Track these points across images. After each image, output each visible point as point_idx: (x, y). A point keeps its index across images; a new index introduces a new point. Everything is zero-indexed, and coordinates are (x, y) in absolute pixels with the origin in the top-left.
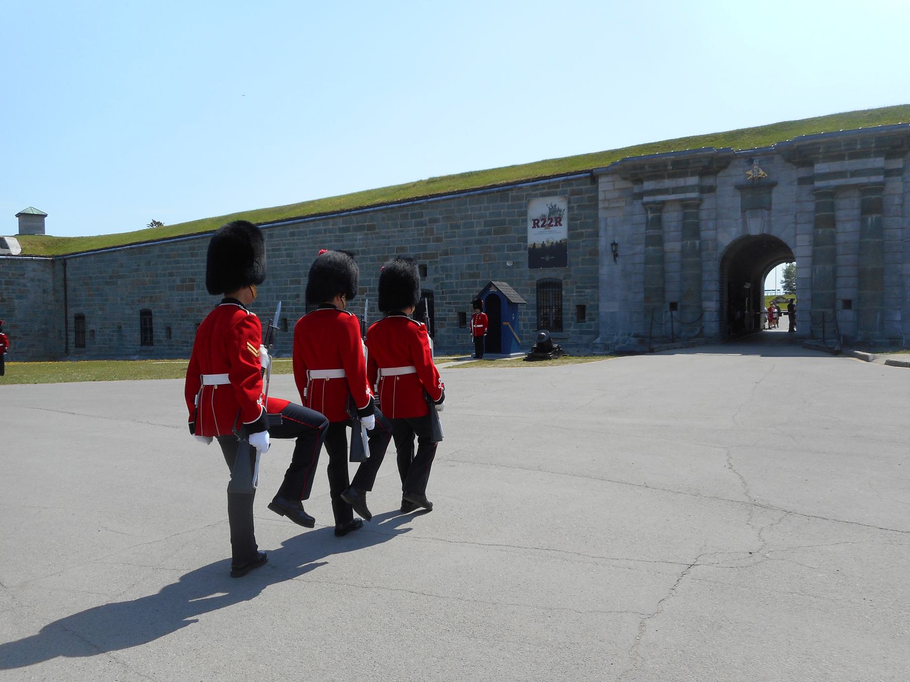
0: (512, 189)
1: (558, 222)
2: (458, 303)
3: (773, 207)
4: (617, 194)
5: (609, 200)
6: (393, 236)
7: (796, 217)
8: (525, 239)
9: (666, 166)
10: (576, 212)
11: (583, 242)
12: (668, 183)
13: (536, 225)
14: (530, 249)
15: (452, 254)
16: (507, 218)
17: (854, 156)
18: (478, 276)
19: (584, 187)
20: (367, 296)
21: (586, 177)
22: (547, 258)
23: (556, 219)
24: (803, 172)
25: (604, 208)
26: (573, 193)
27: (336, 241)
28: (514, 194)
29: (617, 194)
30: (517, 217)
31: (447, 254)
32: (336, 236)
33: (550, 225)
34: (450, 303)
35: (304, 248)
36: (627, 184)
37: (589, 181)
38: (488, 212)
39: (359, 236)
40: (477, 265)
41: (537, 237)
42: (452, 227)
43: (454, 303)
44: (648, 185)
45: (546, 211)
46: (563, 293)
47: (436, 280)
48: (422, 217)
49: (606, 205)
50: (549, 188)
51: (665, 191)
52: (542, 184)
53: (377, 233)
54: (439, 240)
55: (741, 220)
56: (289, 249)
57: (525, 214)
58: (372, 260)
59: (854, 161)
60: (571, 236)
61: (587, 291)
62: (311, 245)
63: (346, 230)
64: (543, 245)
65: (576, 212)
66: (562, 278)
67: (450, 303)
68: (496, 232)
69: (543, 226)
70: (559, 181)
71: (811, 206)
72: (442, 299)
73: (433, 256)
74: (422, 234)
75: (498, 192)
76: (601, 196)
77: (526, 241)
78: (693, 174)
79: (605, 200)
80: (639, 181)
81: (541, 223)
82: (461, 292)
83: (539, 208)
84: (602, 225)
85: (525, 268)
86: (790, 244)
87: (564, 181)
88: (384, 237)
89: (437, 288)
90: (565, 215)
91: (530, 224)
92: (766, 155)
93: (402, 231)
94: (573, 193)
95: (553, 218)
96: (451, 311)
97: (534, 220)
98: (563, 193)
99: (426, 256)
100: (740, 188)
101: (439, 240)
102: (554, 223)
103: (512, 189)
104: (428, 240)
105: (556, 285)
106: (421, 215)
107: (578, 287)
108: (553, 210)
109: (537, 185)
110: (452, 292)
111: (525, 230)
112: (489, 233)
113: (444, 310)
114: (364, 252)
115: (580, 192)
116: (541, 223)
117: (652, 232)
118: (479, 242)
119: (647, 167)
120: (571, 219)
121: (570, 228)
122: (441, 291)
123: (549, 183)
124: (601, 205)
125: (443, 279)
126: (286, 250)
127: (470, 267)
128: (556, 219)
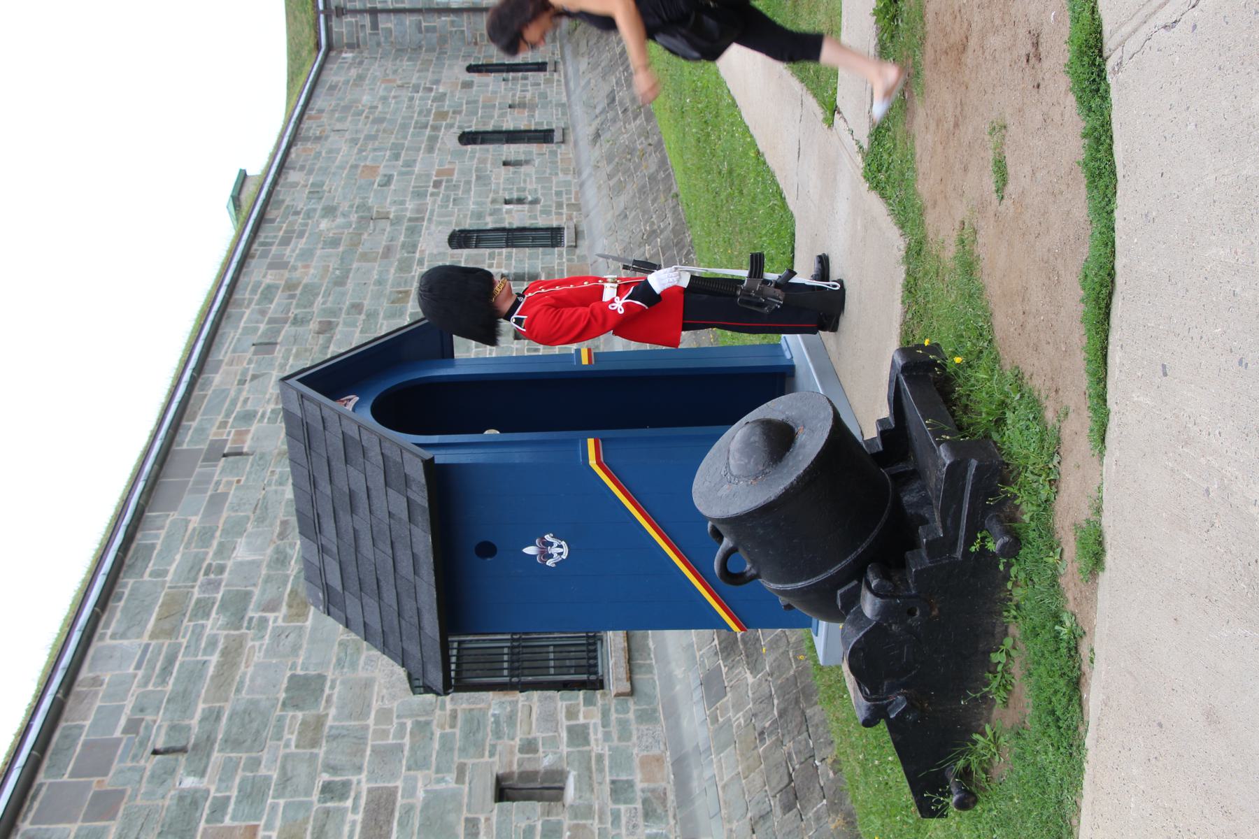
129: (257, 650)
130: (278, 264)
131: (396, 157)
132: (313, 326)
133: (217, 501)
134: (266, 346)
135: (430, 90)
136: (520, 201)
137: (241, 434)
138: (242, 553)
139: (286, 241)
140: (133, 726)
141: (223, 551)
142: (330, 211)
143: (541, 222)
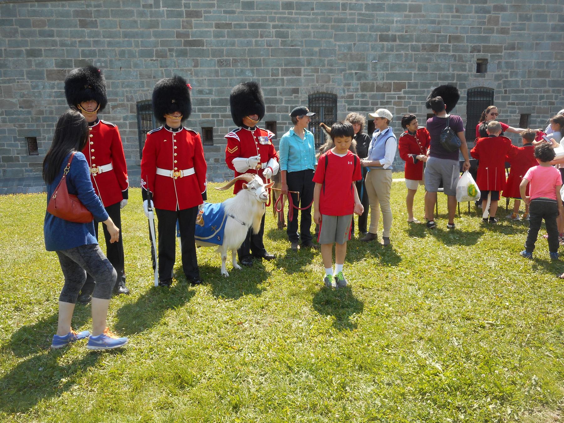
2: (523, 104)
6: (447, 22)
15: (519, 49)
20: (405, 93)
27: (360, 21)
31: (513, 48)
32: (360, 14)
34: (513, 104)
35: (308, 27)
39: (397, 17)
40: (548, 63)
42: (522, 18)
43: (518, 104)
47: (498, 78)
53: (423, 16)
54: (503, 31)
56: (282, 26)
58: (414, 49)
62: (320, 24)
63: (379, 7)
67: (513, 104)
72: (504, 98)
73: (496, 49)
74: (484, 23)
82: (527, 91)
88: (433, 22)
89: (499, 86)
93: (459, 17)
96: (515, 112)
99: (487, 49)
104: (491, 31)
110: (516, 92)
113: (506, 112)
114: (402, 38)
118: (551, 37)
122: (503, 90)
125: (506, 76)
126: (274, 27)
127: (539, 65)
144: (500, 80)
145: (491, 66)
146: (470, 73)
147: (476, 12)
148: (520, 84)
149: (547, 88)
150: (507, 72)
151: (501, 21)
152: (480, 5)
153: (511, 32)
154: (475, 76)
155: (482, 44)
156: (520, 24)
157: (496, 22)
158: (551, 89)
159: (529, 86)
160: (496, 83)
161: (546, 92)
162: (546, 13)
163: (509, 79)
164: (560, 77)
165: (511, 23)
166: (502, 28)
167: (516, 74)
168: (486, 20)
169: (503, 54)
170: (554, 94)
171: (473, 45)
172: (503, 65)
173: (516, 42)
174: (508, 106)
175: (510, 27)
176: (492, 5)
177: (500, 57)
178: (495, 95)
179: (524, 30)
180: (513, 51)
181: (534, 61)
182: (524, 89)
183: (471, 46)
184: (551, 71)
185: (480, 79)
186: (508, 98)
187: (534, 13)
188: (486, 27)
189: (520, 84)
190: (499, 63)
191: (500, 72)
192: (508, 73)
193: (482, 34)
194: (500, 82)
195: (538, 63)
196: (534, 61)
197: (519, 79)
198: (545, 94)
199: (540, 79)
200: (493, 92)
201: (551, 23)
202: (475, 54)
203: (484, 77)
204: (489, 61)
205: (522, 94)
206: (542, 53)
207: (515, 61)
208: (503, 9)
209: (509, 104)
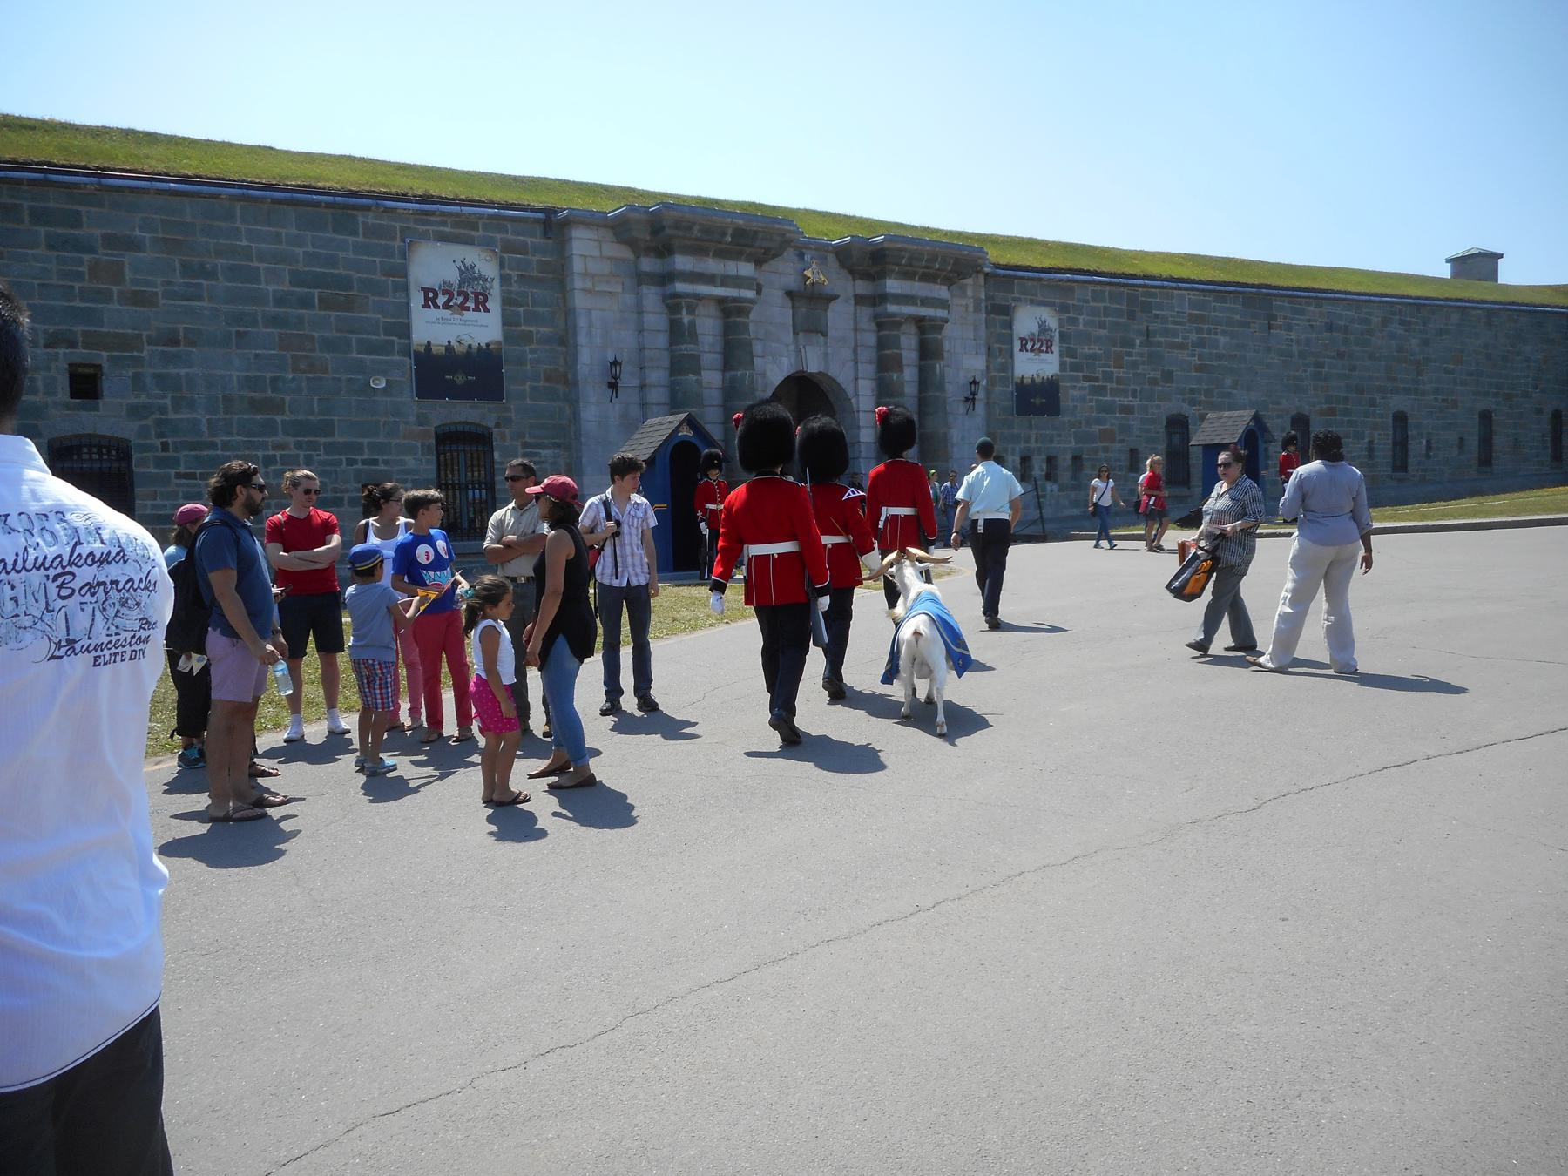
0: (367, 208)
1: (481, 303)
3: (831, 333)
4: (605, 268)
5: (593, 276)
7: (855, 351)
8: (406, 330)
9: (724, 234)
10: (515, 288)
11: (533, 351)
12: (712, 265)
13: (430, 300)
14: (416, 353)
15: (193, 344)
16: (356, 276)
17: (928, 277)
18: (278, 408)
19: (529, 240)
21: (536, 221)
22: (460, 379)
23: (476, 295)
24: (862, 287)
25: (584, 290)
26: (508, 248)
28: (371, 219)
29: (605, 268)
30: (378, 277)
31: (174, 342)
33: (463, 307)
36: (625, 253)
37: (539, 229)
38: (300, 251)
40: (274, 380)
41: (434, 329)
42: (187, 269)
44: (682, 262)
45: (453, 276)
46: (496, 455)
47: (136, 412)
48: (77, 223)
49: (589, 285)
50: (456, 225)
51: (710, 279)
52: (443, 214)
54: (140, 299)
55: (792, 347)
57: (404, 273)
59: (922, 284)
60: (508, 337)
61: (543, 452)
64: (449, 348)
65: (515, 288)
66: (491, 424)
68: (326, 304)
69: (446, 306)
70: (481, 216)
71: (871, 339)
75: (329, 205)
76: (578, 266)
77: (409, 337)
78: (748, 260)
79: (585, 275)
80: (664, 250)
81: (441, 300)
83: (435, 264)
84: (582, 322)
85: (407, 397)
86: (850, 391)
87: (491, 217)
90: (496, 291)
91: (417, 299)
92: (823, 250)
94: (508, 248)
95: (465, 294)
97: (426, 291)
98: (486, 243)
99: (93, 341)
100: (789, 294)
101: (140, 299)
102: (471, 304)
103: (367, 208)
105: (480, 439)
106: (75, 220)
107: (525, 445)
108: (468, 274)
109: (432, 213)
110: (195, 446)
111: (406, 309)
112: (305, 303)
115: (521, 249)
116: (441, 300)
117: (686, 348)
118: (274, 321)
119: (696, 228)
120: (506, 301)
121: (507, 321)
122: (158, 442)
123: (457, 215)
124: (578, 283)
125: (162, 409)
128: (476, 295)
129: (1183, 355)
130: (1385, 322)
131: (1471, 374)
132: (1343, 349)
133: (1246, 324)
134: (1330, 327)
135: (1536, 387)
136: (1429, 447)
137: (1280, 327)
138: (1223, 340)
139: (1402, 322)
140: (1157, 316)
141: (1224, 333)
142: (1425, 343)
143: (1412, 461)
144: (146, 418)
145: (113, 384)
146: (49, 400)
147: (51, 247)
148: (204, 428)
149: (281, 438)
150: (164, 397)
151: (128, 275)
152: (60, 231)
153: (162, 302)
154: (68, 407)
155: (80, 328)
156: (187, 285)
157: (117, 275)
158: (291, 440)
159: (230, 433)
160: (135, 425)
161: (277, 447)
162: (256, 264)
163: (172, 416)
164: (312, 413)
165: (159, 280)
166: (135, 293)
167: (191, 405)
168: (84, 269)
169: (145, 354)
170: (302, 453)
171: (52, 329)
172: (148, 380)
173: (181, 327)
174: (175, 481)
175: (159, 290)
176: (98, 232)
177: (138, 361)
178: (135, 456)
179: (200, 298)
180: (175, 349)
181: (235, 374)
182: (217, 440)
183: (45, 332)
184: (287, 399)
185: (84, 413)
186: (175, 462)
187: (221, 261)
188: (86, 285)
189: (204, 428)
190: (137, 378)
191: (143, 399)
192: (168, 401)
193: (78, 304)
194: (144, 422)
195: (247, 378)
196: (235, 374)
197: (202, 417)
198: (278, 454)
199: (259, 417)
200: (129, 448)
201: (271, 288)
202: (61, 351)
203: (97, 409)
204: (105, 370)
205: (211, 453)
206: (257, 356)
207: (183, 372)
208: (133, 245)
209: (179, 476)
